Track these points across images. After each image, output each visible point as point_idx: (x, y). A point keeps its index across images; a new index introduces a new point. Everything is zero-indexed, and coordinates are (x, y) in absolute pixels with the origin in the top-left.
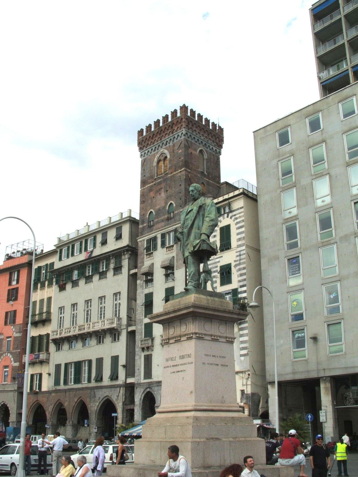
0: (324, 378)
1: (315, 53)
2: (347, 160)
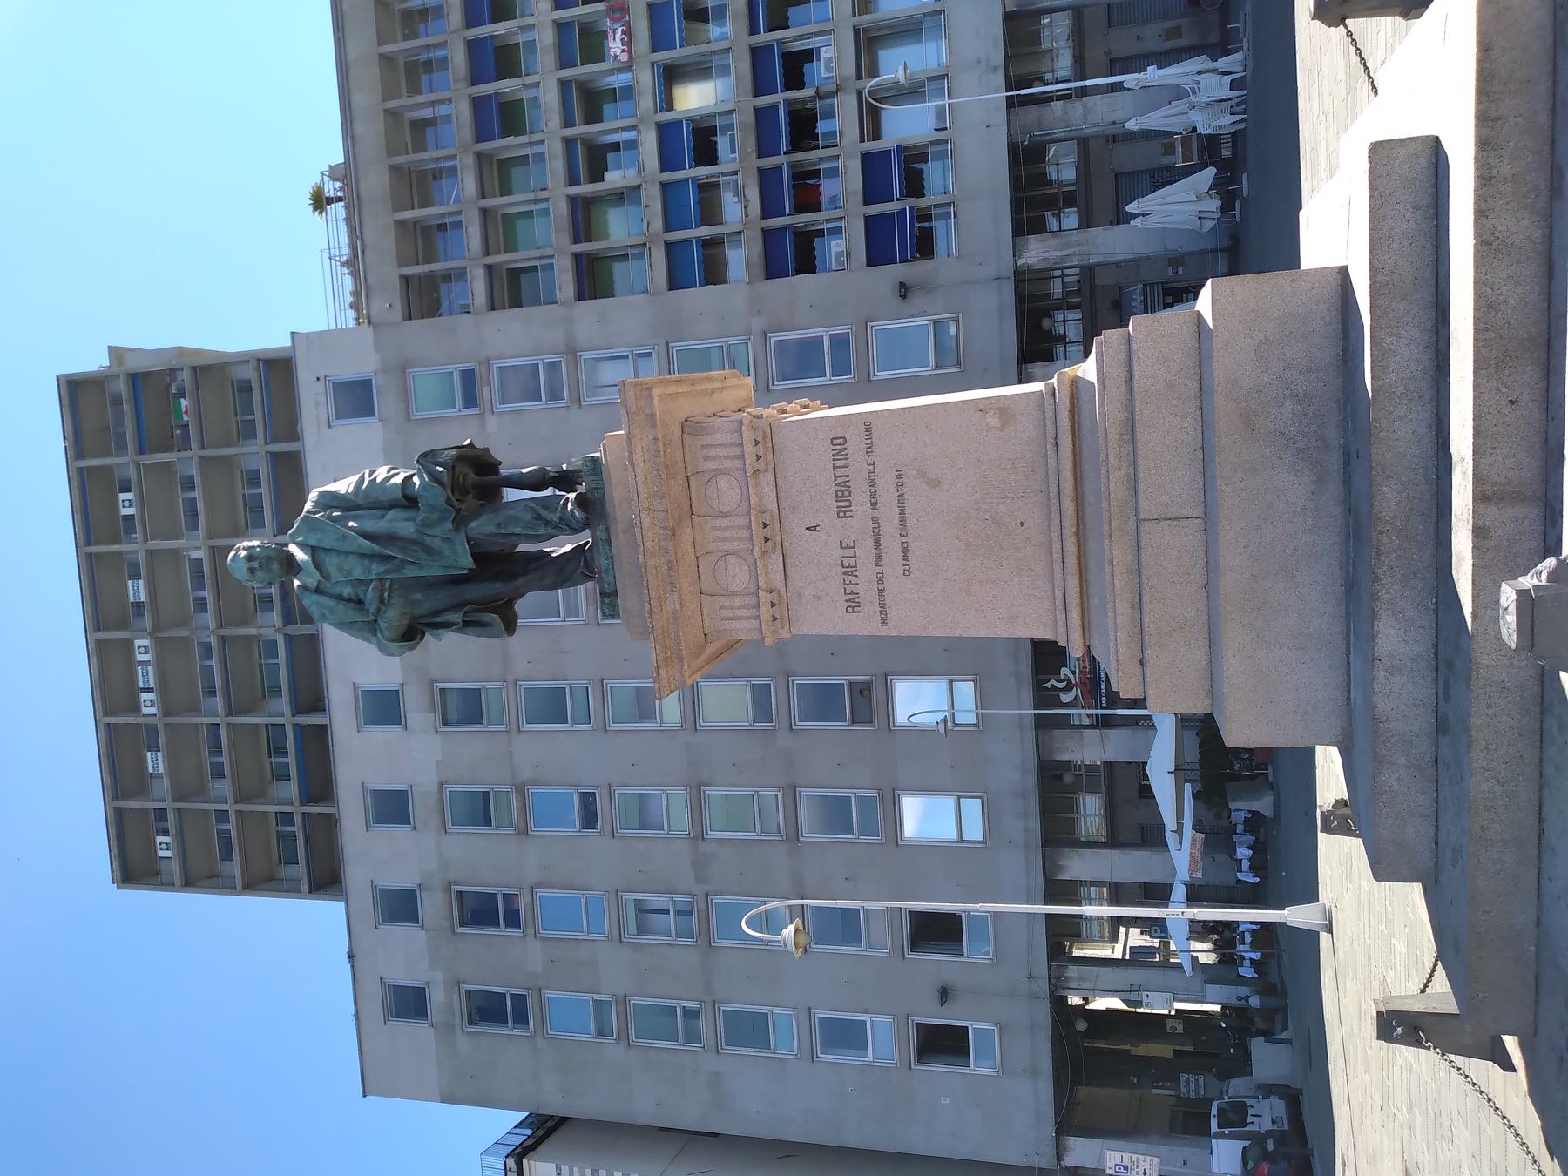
0: (1053, 981)
1: (231, 894)
2: (513, 832)
